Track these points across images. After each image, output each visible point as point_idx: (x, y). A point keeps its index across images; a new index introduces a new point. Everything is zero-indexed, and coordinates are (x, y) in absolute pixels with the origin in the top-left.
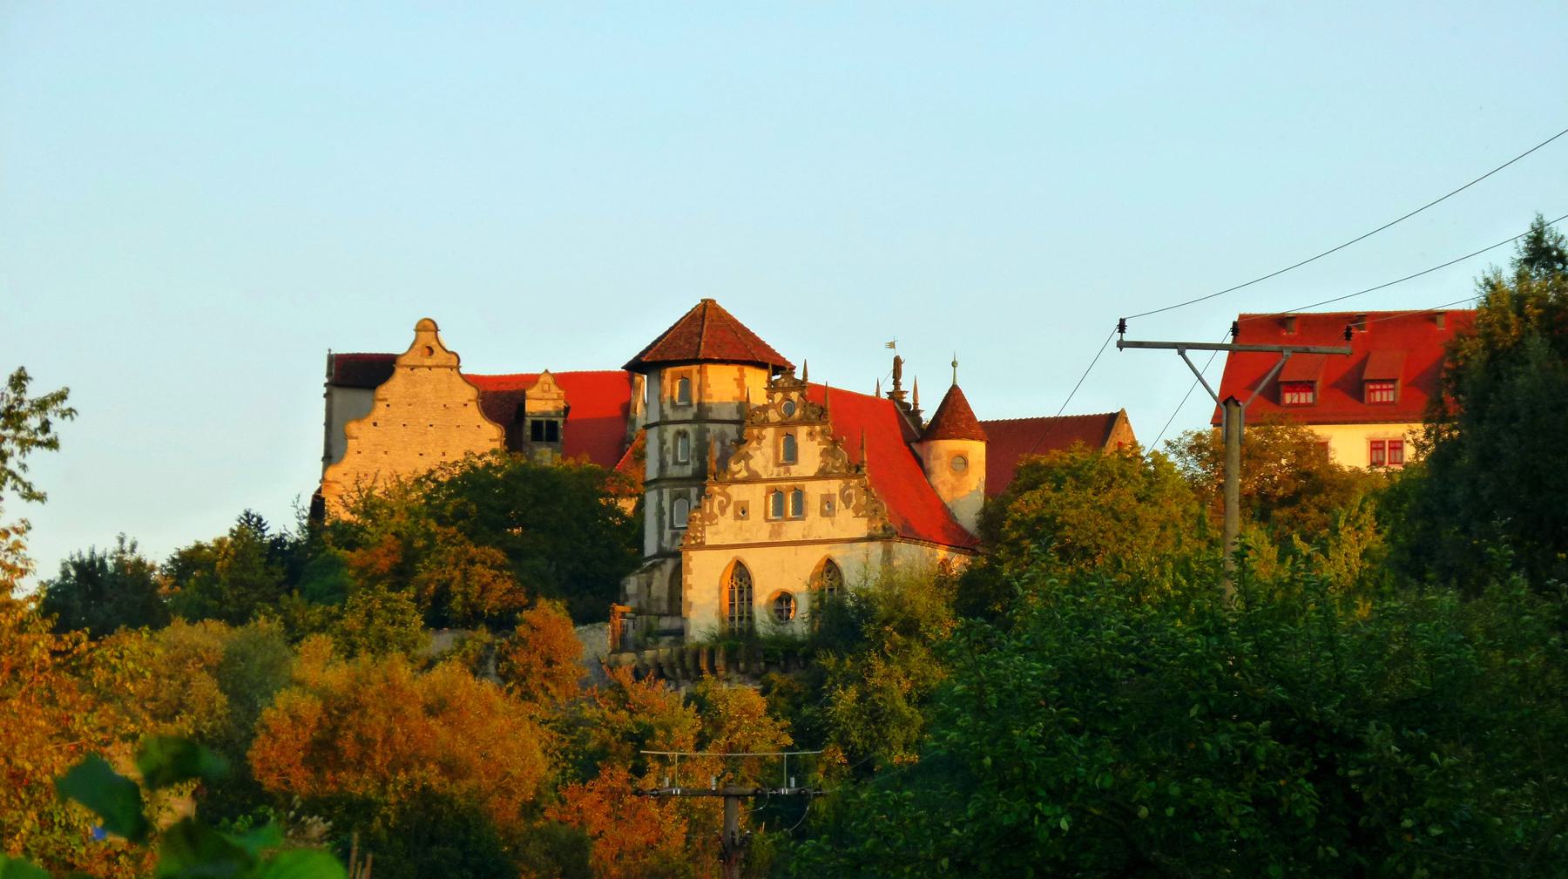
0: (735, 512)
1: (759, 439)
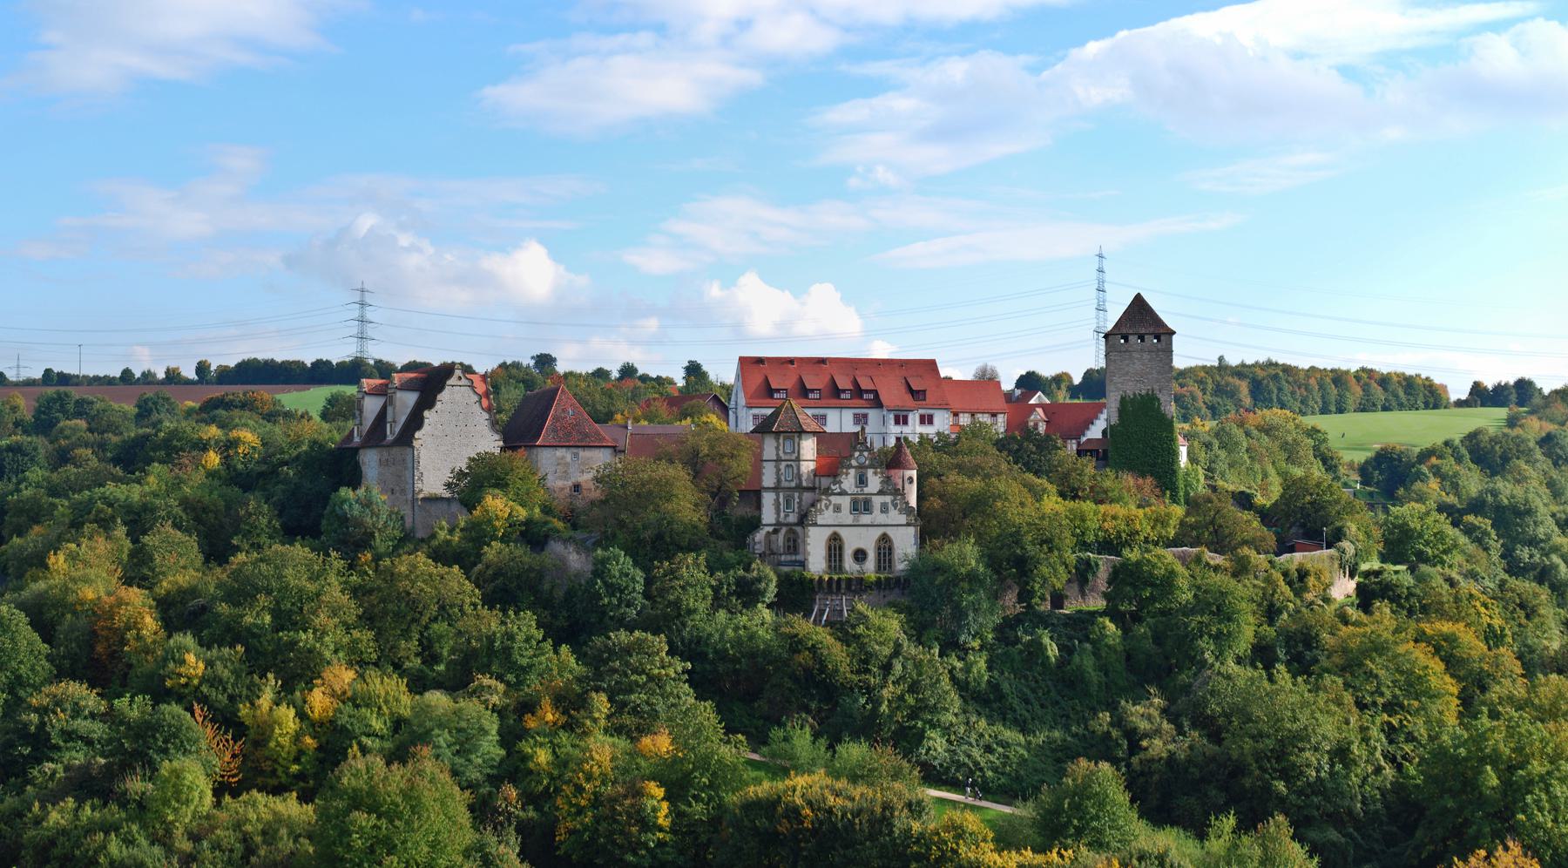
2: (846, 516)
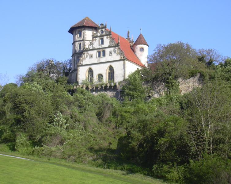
0: (90, 57)
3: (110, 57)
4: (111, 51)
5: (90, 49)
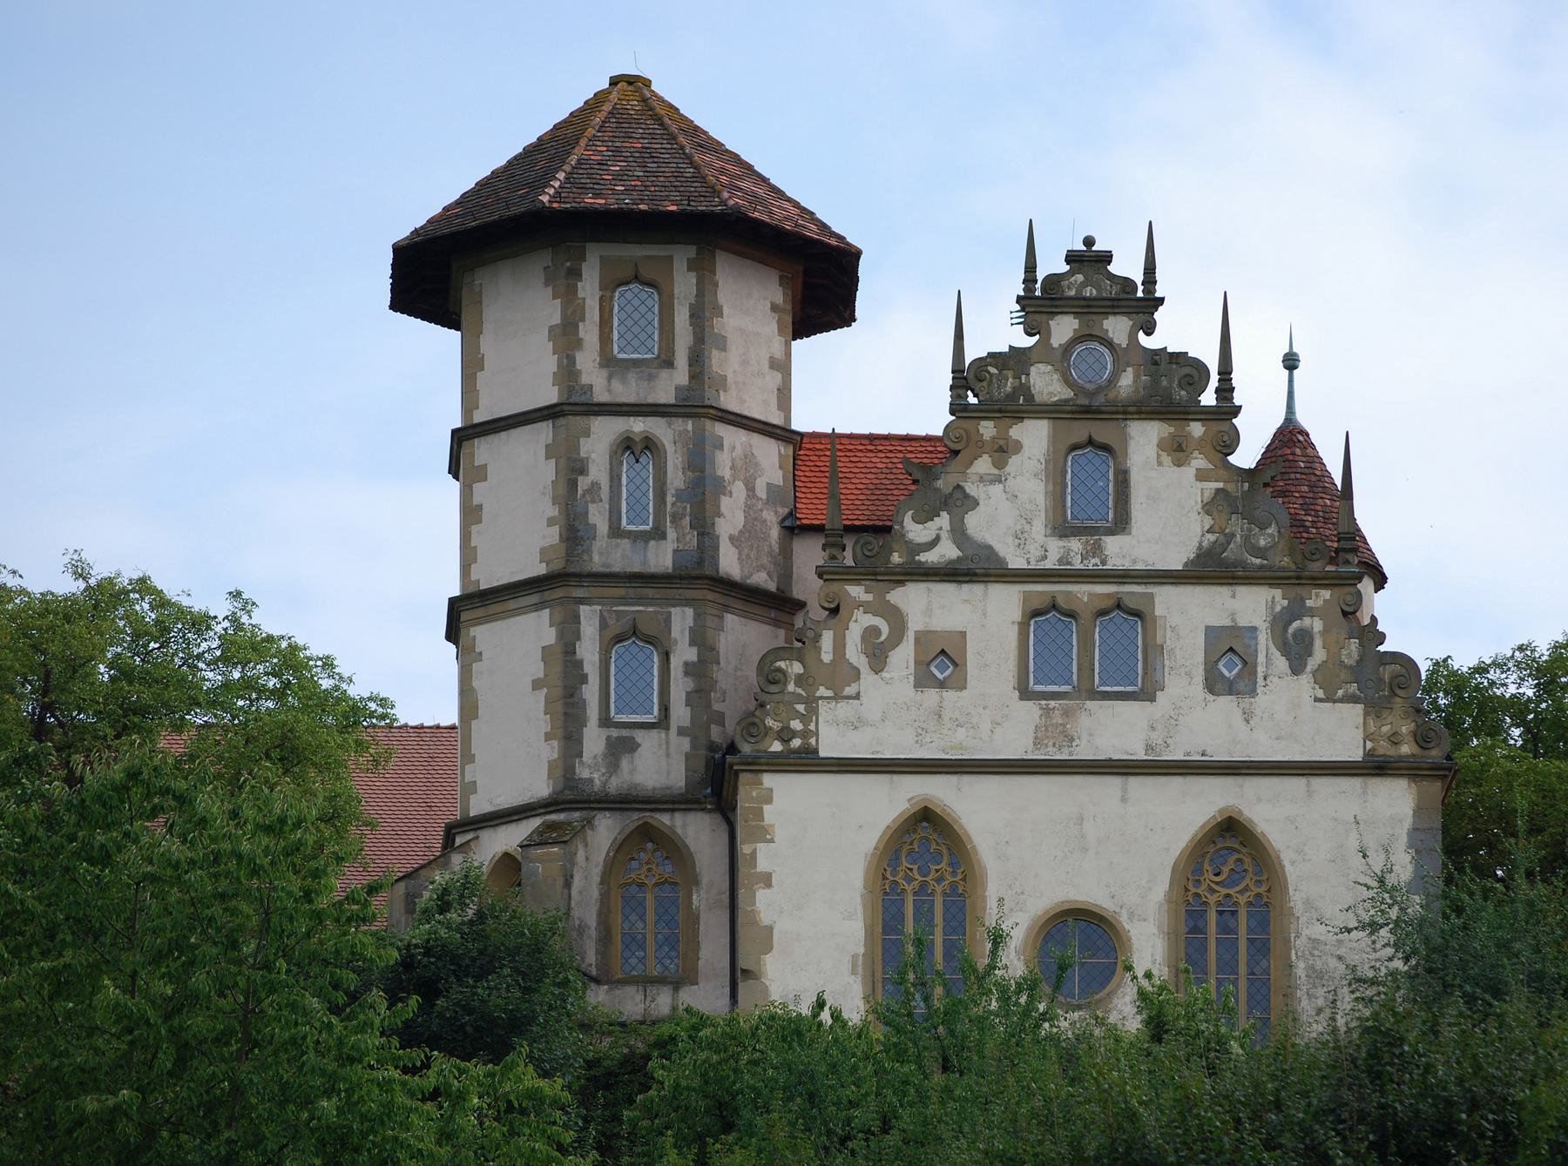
1: (1003, 451)
2: (990, 713)
3: (1226, 704)
4: (1234, 630)
5: (930, 557)
